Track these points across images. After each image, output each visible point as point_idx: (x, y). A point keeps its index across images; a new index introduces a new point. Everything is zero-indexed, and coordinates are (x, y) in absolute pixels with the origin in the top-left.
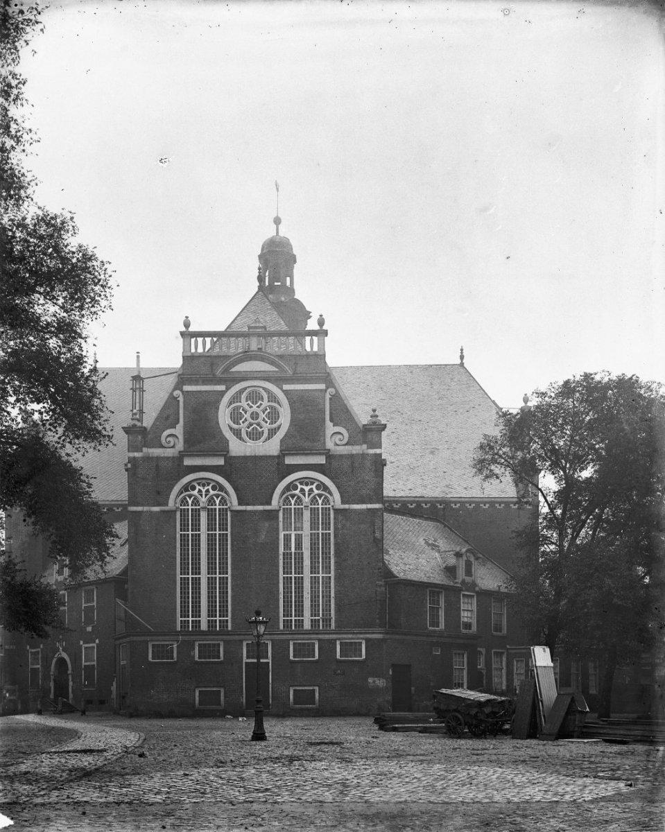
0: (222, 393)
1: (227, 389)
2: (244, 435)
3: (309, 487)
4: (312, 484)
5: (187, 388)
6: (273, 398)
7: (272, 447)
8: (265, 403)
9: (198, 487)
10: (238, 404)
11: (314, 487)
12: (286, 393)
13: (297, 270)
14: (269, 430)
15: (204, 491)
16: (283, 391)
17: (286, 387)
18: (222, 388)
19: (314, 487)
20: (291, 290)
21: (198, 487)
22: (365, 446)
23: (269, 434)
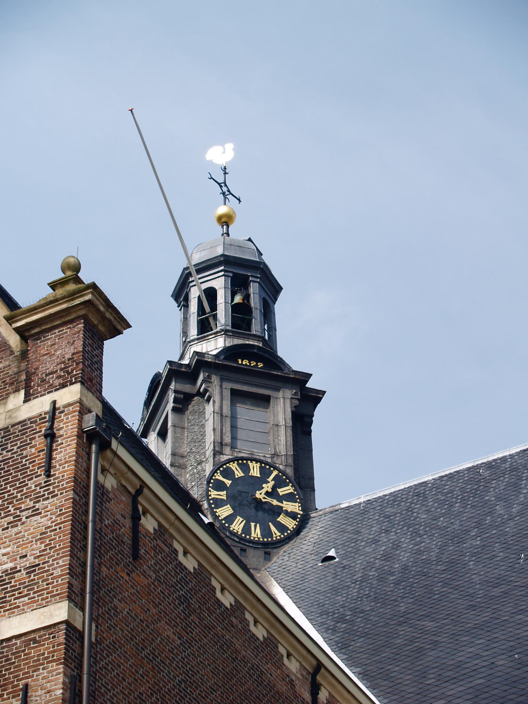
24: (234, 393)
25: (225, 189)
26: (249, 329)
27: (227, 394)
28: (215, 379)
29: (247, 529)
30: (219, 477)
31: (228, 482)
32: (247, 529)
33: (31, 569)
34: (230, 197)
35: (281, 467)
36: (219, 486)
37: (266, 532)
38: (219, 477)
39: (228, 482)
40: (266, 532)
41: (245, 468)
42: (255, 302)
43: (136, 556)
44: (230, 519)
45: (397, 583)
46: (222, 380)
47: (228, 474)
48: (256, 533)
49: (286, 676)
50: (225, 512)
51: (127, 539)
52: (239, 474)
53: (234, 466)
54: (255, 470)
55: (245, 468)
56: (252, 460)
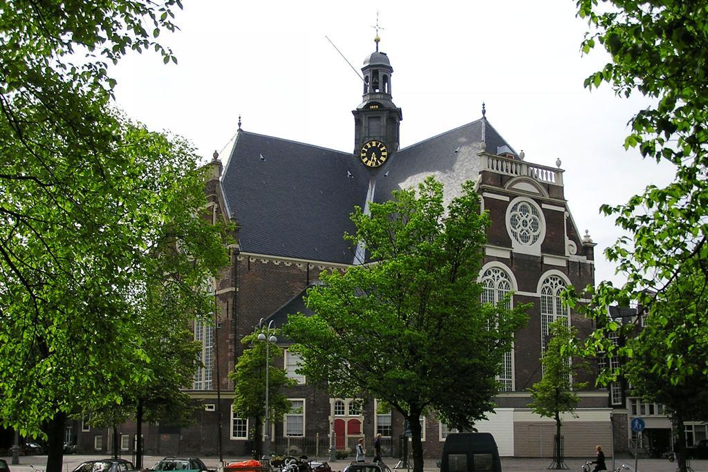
13: (394, 79)
20: (389, 96)
24: (369, 118)
25: (377, 28)
27: (367, 119)
28: (363, 116)
30: (364, 149)
31: (366, 150)
36: (364, 152)
38: (364, 149)
39: (366, 150)
41: (371, 144)
44: (367, 162)
46: (365, 115)
47: (366, 147)
50: (366, 159)
52: (369, 146)
55: (371, 144)
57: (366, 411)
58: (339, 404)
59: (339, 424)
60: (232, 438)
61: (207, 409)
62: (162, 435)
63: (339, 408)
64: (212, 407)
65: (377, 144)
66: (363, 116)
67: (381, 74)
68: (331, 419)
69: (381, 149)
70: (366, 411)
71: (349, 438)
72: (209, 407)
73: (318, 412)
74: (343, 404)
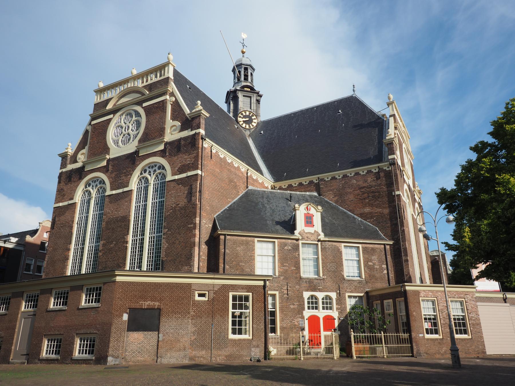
0: (110, 120)
1: (114, 116)
2: (120, 143)
3: (154, 169)
4: (156, 166)
5: (94, 122)
6: (138, 114)
7: (131, 148)
8: (134, 118)
9: (92, 184)
10: (119, 124)
11: (156, 168)
12: (145, 108)
14: (133, 135)
15: (94, 185)
16: (143, 108)
17: (145, 105)
18: (111, 116)
19: (156, 168)
21: (92, 184)
22: (190, 130)
23: (133, 139)
25: (243, 44)
26: (248, 80)
29: (246, 126)
32: (246, 126)
33: (192, 164)
34: (244, 46)
35: (253, 112)
37: (250, 127)
40: (250, 127)
41: (245, 113)
42: (249, 74)
43: (211, 158)
45: (273, 140)
48: (247, 127)
49: (242, 173)
51: (210, 156)
53: (243, 113)
54: (248, 113)
55: (245, 113)
56: (247, 111)
57: (339, 307)
58: (312, 299)
59: (313, 320)
60: (231, 336)
61: (197, 298)
62: (131, 333)
63: (312, 303)
64: (203, 295)
65: (250, 114)
66: (239, 93)
67: (250, 71)
68: (307, 313)
69: (253, 118)
70: (339, 307)
71: (325, 337)
72: (200, 295)
73: (292, 307)
74: (316, 298)
